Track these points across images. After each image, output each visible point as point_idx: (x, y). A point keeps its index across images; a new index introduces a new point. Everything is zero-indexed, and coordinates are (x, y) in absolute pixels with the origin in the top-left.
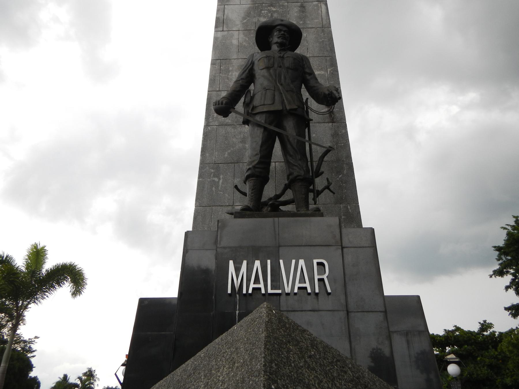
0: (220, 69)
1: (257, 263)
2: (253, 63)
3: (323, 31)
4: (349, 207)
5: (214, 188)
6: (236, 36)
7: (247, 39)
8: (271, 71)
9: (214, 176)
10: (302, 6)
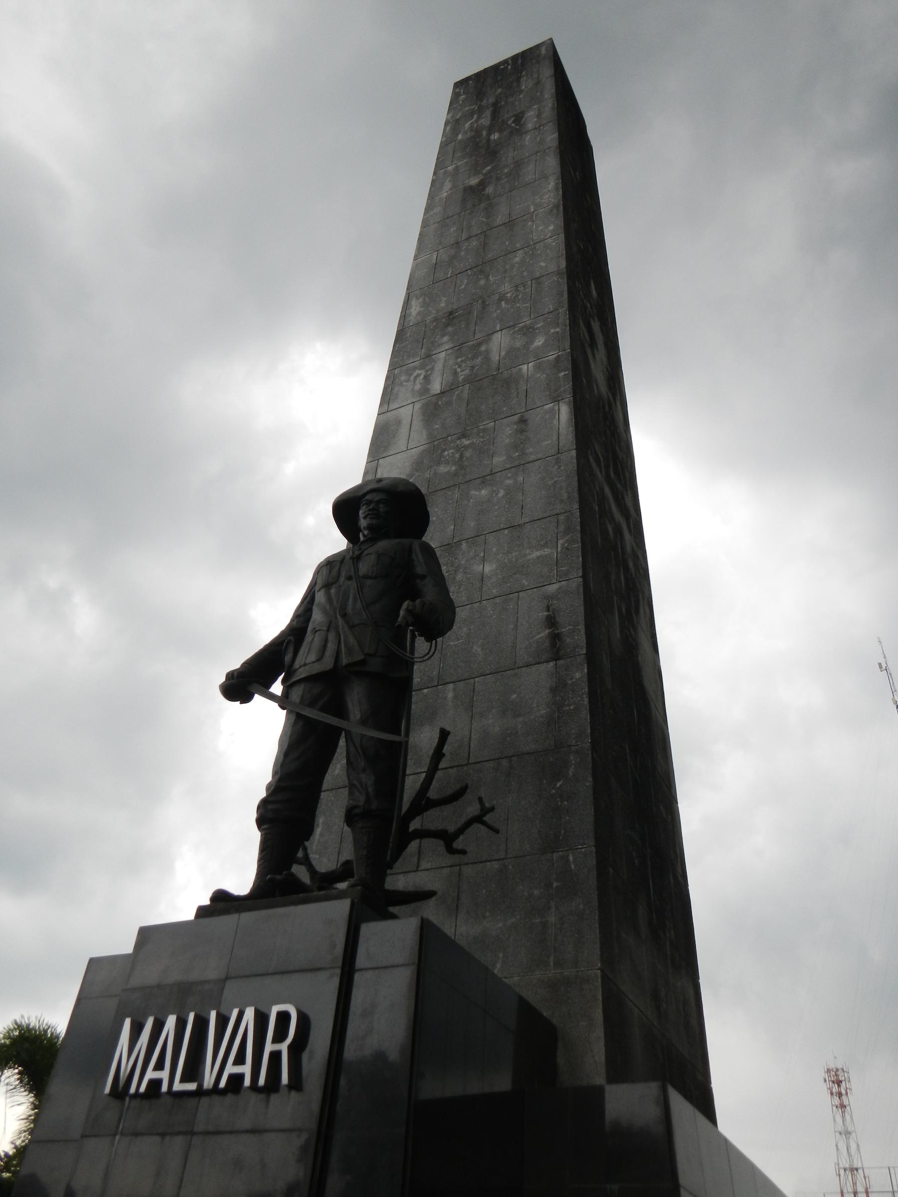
4: (571, 858)
8: (333, 591)
10: (523, 421)
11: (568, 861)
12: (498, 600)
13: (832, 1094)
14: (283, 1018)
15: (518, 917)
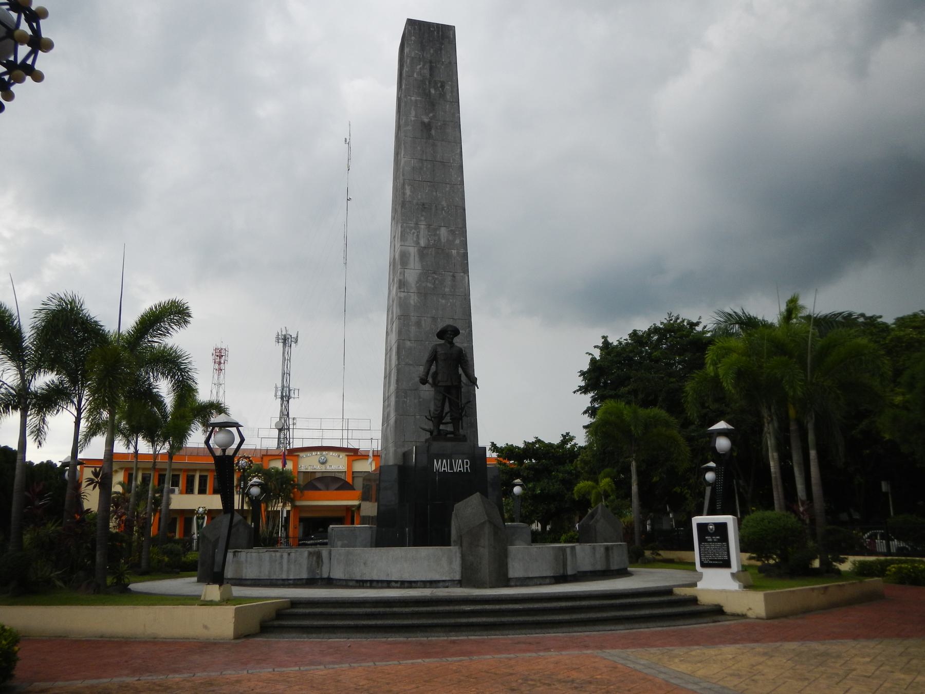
2: (436, 352)
10: (454, 276)
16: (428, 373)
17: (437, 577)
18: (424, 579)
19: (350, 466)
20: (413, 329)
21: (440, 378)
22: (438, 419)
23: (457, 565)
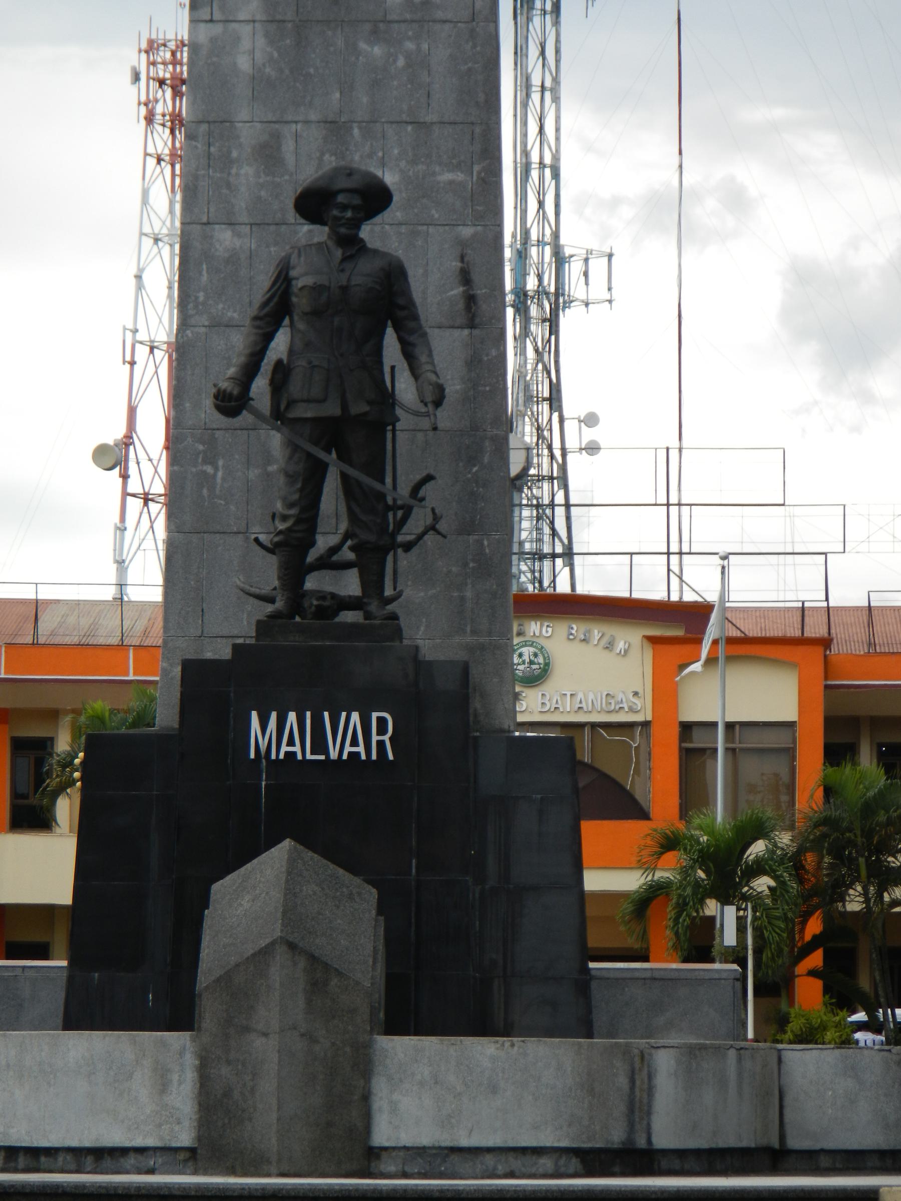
0: (209, 154)
1: (292, 717)
3: (473, 34)
4: (486, 543)
5: (205, 492)
6: (246, 44)
7: (276, 55)
9: (205, 462)
11: (482, 544)
12: (403, 229)
13: (150, 119)
14: (382, 722)
15: (438, 589)
16: (251, 370)
17: (115, 1137)
18: (74, 1143)
19: (665, 690)
20: (246, 174)
21: (296, 387)
22: (293, 548)
23: (183, 1097)
